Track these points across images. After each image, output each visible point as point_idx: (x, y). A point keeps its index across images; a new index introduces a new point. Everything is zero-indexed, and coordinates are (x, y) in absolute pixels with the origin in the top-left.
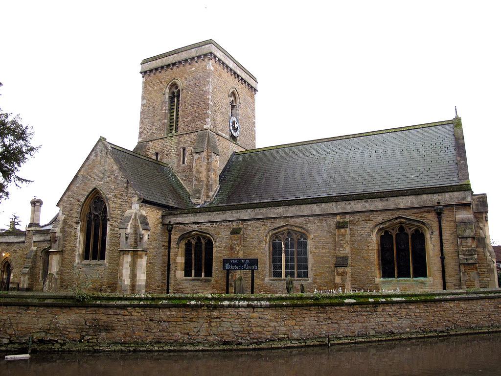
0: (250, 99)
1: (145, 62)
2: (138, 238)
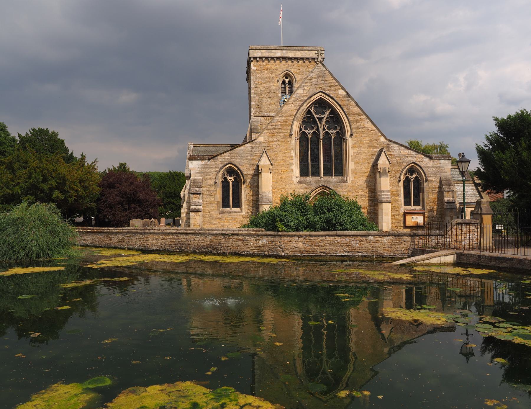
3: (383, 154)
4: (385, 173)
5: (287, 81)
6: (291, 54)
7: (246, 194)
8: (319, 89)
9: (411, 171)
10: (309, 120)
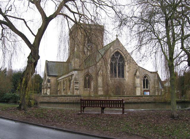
3: (138, 71)
4: (138, 77)
7: (92, 84)
9: (145, 77)
10: (113, 58)
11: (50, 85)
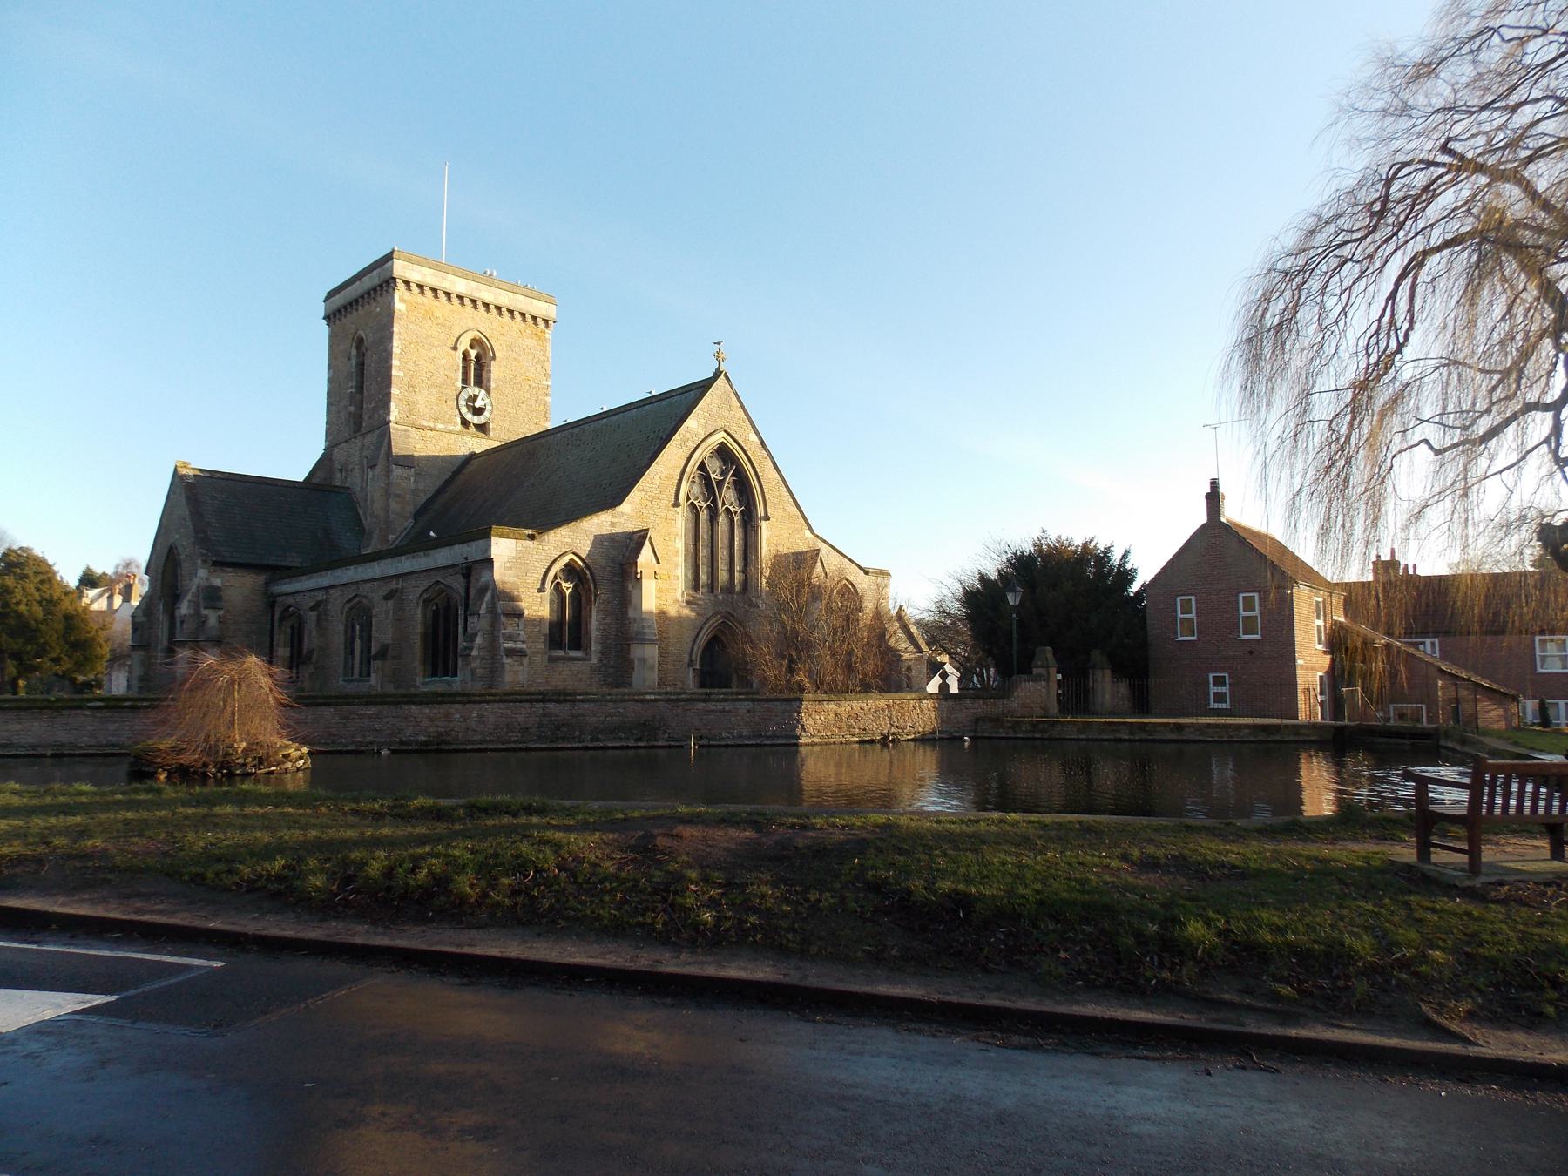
0: (532, 343)
1: (331, 294)
2: (202, 622)
5: (473, 353)
6: (486, 294)
8: (720, 424)
11: (220, 620)
